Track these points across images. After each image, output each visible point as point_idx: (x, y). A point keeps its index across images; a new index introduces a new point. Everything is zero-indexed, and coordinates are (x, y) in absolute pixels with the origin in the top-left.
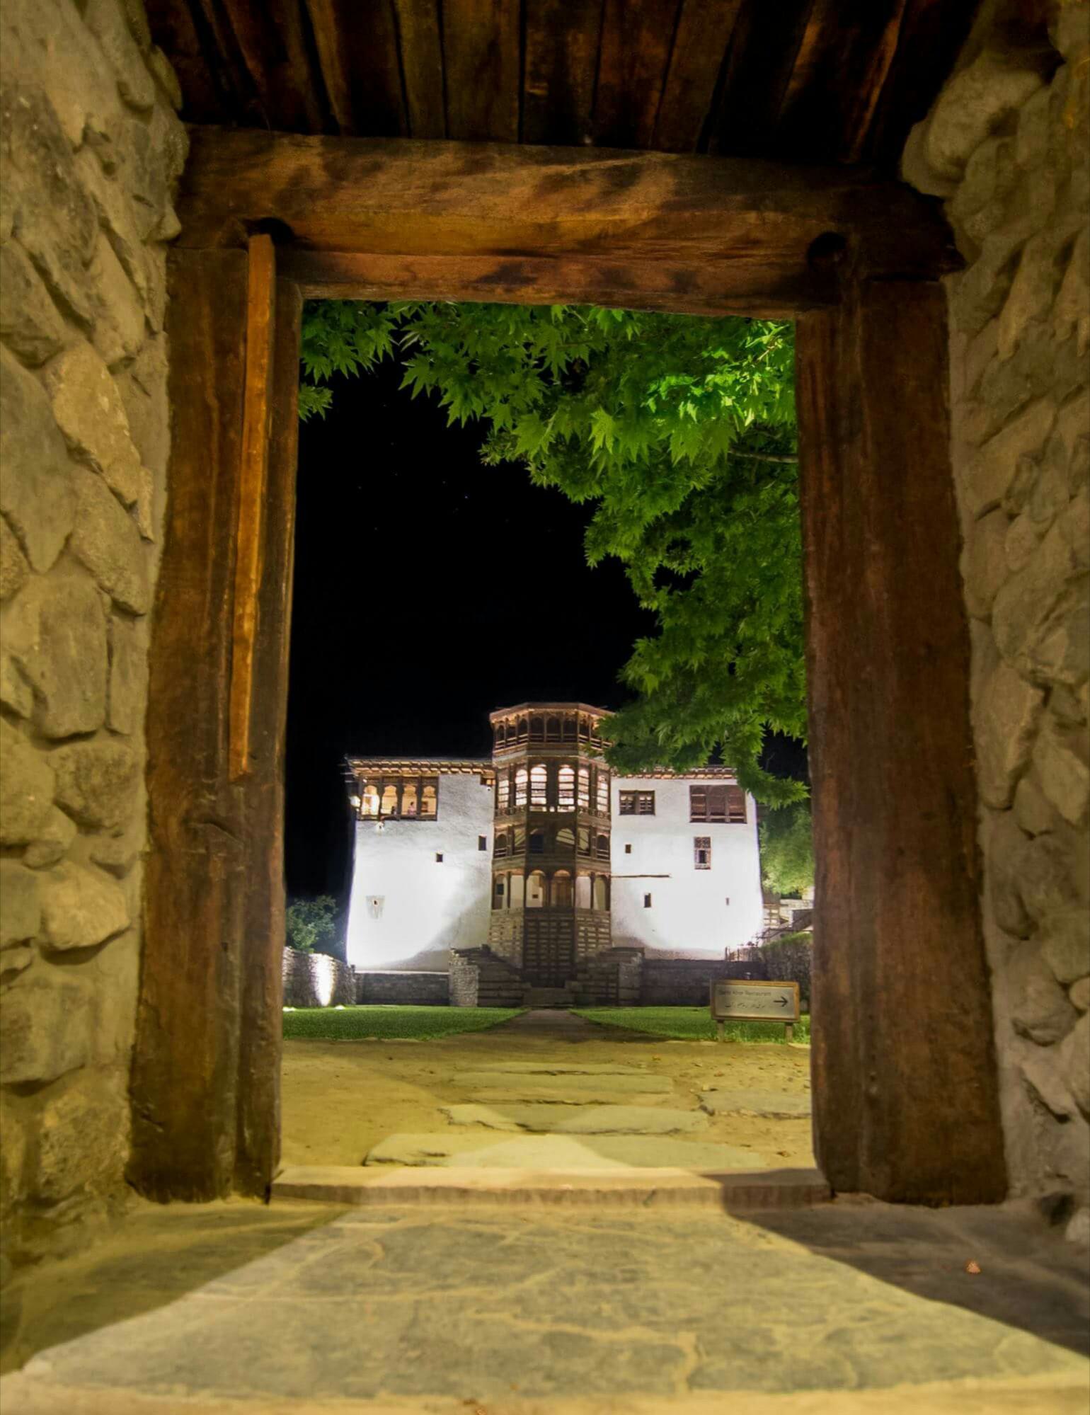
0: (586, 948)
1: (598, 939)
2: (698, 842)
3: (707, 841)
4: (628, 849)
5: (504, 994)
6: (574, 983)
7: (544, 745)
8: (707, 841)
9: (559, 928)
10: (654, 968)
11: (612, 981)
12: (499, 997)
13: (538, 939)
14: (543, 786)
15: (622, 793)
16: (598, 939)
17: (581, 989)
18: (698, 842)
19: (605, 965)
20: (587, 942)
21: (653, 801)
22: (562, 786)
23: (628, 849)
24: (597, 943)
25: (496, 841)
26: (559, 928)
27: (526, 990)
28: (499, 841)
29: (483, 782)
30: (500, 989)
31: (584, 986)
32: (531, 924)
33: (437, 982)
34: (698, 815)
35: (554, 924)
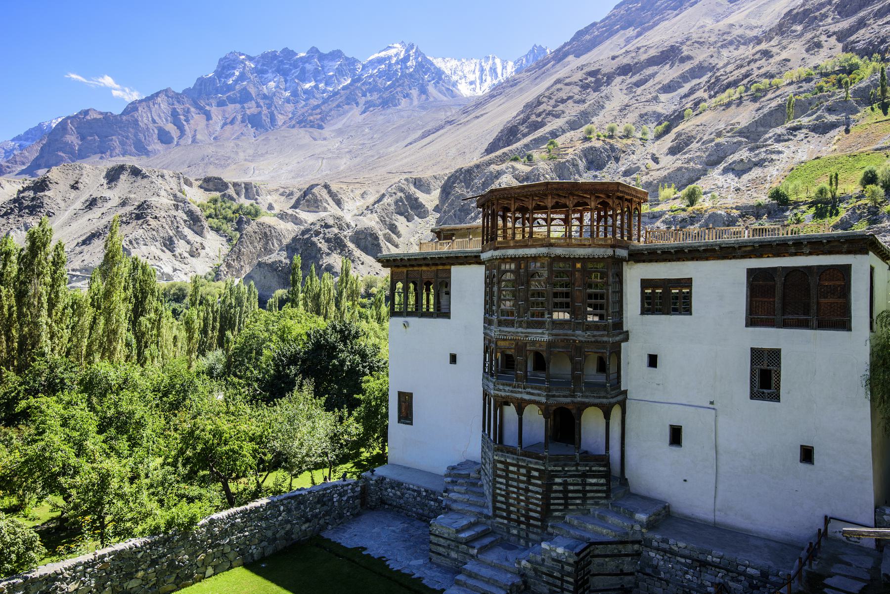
0: (566, 505)
1: (584, 492)
2: (757, 354)
3: (775, 355)
4: (653, 361)
5: (454, 555)
8: (775, 355)
9: (529, 477)
10: (658, 549)
11: (569, 574)
12: (448, 556)
16: (584, 492)
17: (532, 573)
18: (757, 354)
20: (566, 498)
21: (690, 294)
23: (653, 361)
24: (584, 499)
26: (529, 477)
30: (449, 547)
31: (535, 570)
32: (499, 465)
33: (436, 500)
34: (757, 316)
35: (523, 471)
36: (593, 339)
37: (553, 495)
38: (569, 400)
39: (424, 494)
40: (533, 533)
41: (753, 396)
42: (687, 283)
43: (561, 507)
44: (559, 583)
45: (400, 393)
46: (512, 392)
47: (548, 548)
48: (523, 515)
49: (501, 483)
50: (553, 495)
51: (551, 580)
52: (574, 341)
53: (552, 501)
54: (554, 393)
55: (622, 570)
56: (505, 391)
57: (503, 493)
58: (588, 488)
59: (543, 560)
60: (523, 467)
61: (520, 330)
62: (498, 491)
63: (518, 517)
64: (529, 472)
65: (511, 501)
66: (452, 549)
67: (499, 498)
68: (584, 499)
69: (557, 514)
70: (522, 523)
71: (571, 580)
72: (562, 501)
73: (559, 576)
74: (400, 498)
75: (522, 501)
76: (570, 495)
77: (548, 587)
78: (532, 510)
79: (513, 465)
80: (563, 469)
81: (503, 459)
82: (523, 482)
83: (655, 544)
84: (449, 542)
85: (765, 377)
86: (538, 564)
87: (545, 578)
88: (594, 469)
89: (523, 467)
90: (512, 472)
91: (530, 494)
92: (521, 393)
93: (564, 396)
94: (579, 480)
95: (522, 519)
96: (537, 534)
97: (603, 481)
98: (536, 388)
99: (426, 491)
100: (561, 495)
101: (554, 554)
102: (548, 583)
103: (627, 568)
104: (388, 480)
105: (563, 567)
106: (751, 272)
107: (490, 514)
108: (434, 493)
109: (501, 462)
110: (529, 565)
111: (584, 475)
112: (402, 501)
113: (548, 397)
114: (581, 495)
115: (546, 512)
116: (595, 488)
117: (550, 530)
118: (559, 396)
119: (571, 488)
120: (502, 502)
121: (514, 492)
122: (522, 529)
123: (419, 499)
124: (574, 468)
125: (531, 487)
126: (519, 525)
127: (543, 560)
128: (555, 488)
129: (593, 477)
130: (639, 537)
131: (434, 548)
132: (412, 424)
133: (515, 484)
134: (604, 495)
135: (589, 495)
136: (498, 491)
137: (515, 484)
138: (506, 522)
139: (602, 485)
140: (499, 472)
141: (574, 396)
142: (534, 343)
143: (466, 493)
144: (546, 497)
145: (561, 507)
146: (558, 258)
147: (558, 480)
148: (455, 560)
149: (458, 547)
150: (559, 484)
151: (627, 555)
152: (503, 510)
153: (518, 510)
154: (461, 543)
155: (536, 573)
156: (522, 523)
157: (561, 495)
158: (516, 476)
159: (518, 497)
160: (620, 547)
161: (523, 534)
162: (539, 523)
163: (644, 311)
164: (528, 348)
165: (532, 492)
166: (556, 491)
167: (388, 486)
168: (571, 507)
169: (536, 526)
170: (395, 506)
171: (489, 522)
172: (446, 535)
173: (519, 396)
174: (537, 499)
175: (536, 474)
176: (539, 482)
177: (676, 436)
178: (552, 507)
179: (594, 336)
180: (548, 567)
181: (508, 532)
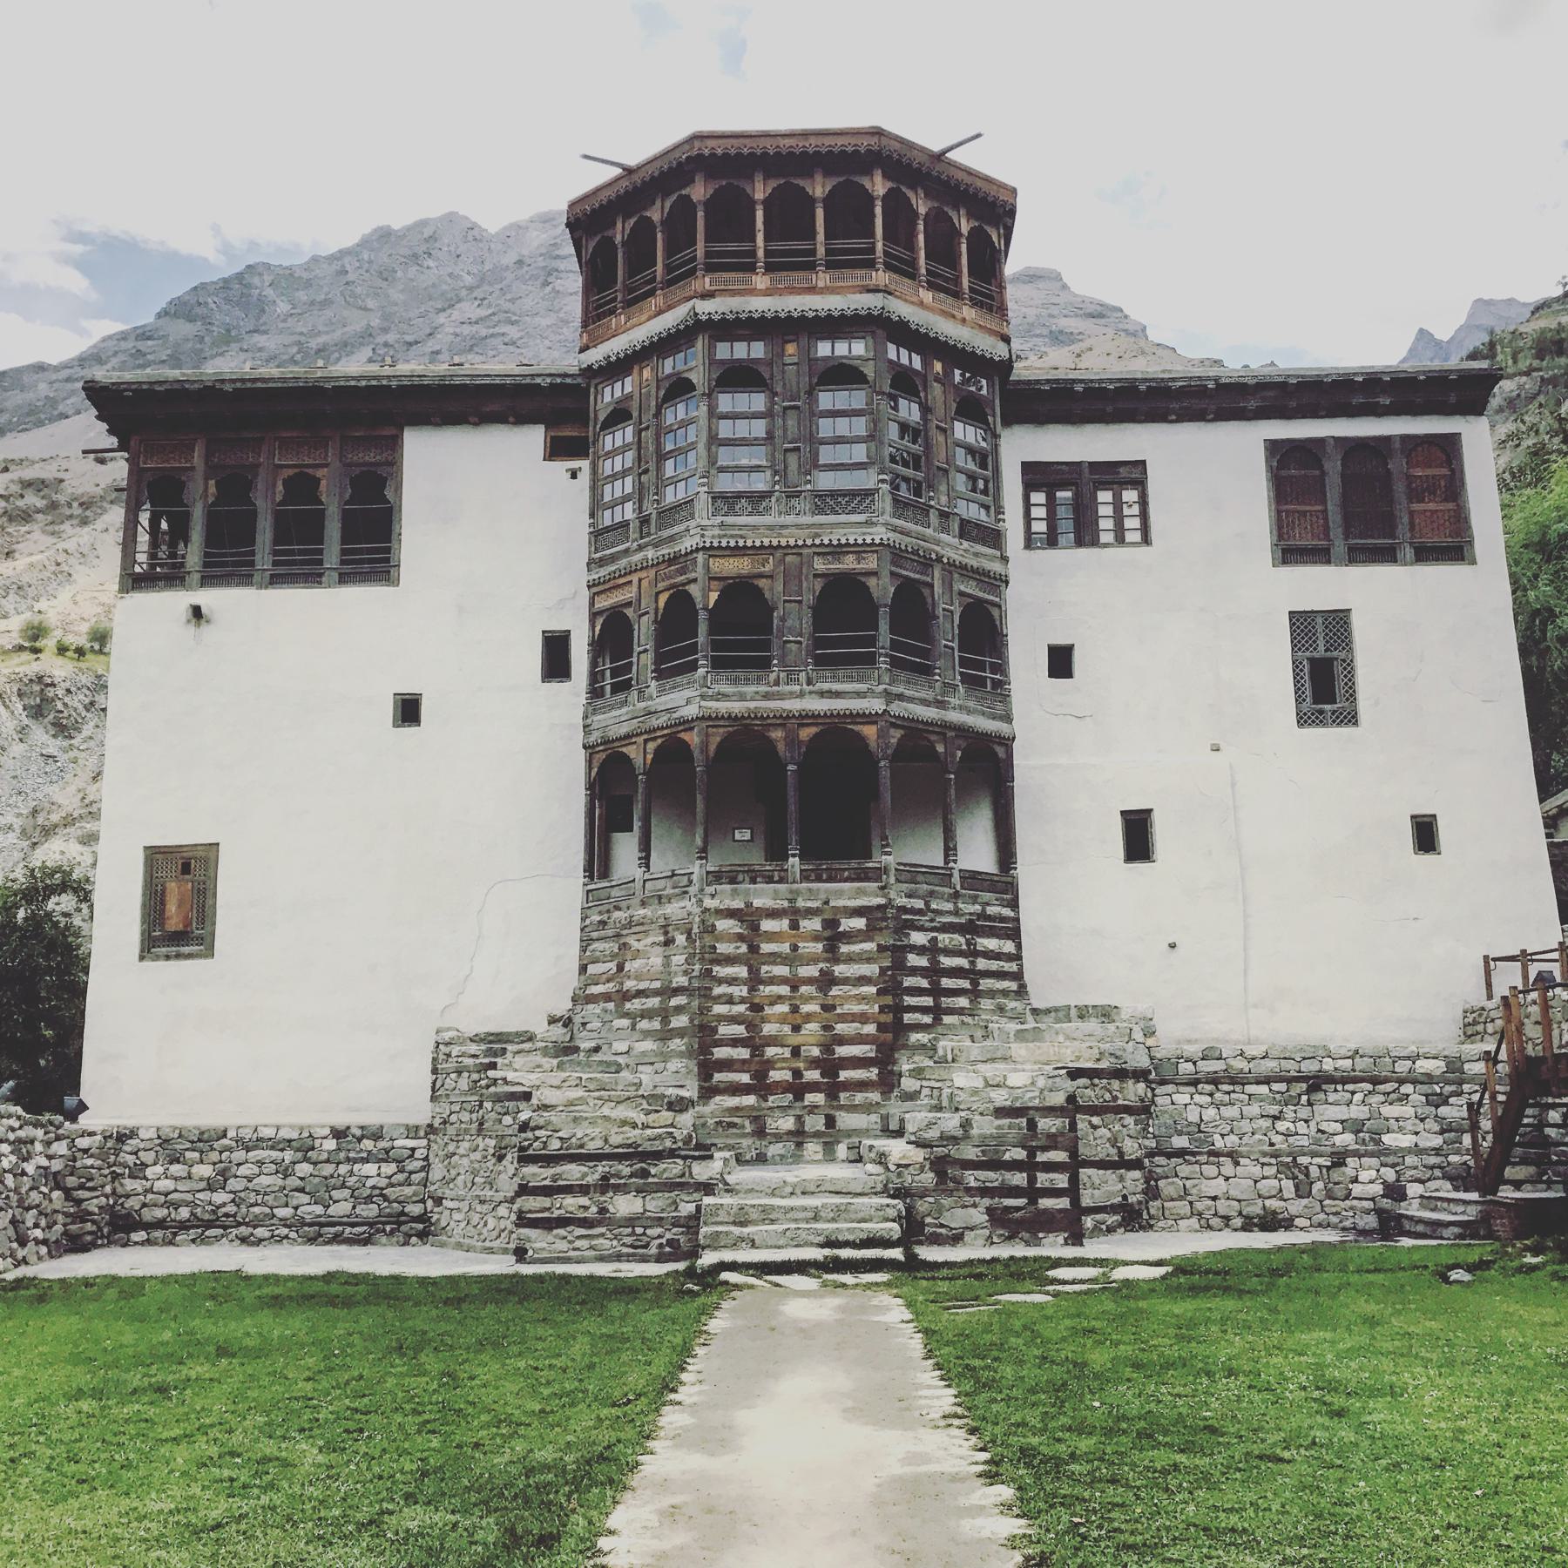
0: (937, 1012)
2: (1302, 623)
5: (625, 1205)
6: (898, 1149)
7: (761, 281)
9: (833, 938)
10: (1194, 1083)
11: (1052, 1142)
13: (755, 981)
14: (759, 428)
15: (1037, 475)
16: (973, 975)
17: (929, 1178)
18: (1302, 623)
19: (1017, 1079)
20: (936, 991)
22: (825, 428)
23: (1061, 662)
24: (975, 994)
25: (598, 648)
27: (707, 1188)
28: (612, 635)
29: (557, 450)
30: (605, 1185)
31: (940, 1165)
32: (723, 925)
33: (386, 1157)
35: (815, 924)
36: (974, 562)
37: (909, 982)
38: (930, 713)
39: (331, 1144)
40: (853, 1108)
41: (1303, 720)
42: (1131, 475)
43: (927, 1019)
44: (1019, 1179)
45: (155, 856)
46: (767, 696)
47: (980, 1084)
48: (814, 1063)
49: (732, 981)
50: (909, 982)
51: (992, 1177)
52: (939, 559)
53: (909, 1000)
54: (900, 689)
55: (1121, 1153)
56: (742, 697)
57: (741, 1008)
58: (982, 964)
59: (966, 1125)
60: (811, 913)
61: (790, 519)
62: (719, 1009)
63: (797, 1073)
64: (831, 924)
65: (769, 1029)
66: (617, 1189)
67: (725, 1030)
68: (975, 994)
69: (915, 1037)
70: (814, 1087)
71: (1059, 1156)
72: (928, 1001)
73: (1020, 1154)
74: (211, 1188)
75: (809, 1017)
76: (946, 983)
77: (986, 1202)
78: (842, 1041)
79: (773, 914)
80: (927, 904)
81: (738, 904)
82: (813, 960)
83: (1186, 1068)
84: (602, 1168)
85: (1324, 679)
86: (955, 1140)
87: (971, 1178)
88: (991, 910)
89: (811, 913)
90: (772, 937)
91: (835, 991)
92: (801, 695)
93: (925, 702)
94: (959, 940)
95: (813, 1075)
96: (868, 1108)
97: (1009, 947)
98: (850, 679)
99: (339, 1134)
100: (924, 983)
101: (1000, 1098)
102: (984, 1191)
103: (1131, 1148)
104: (143, 1134)
105: (1032, 1125)
106: (1273, 447)
107: (691, 1092)
108: (377, 1136)
109: (731, 914)
110: (918, 1155)
111: (970, 928)
112: (220, 1197)
113: (889, 697)
114: (966, 984)
115: (893, 1035)
116: (994, 965)
117: (908, 1084)
118: (911, 700)
119: (947, 962)
120: (735, 1042)
121: (779, 999)
122: (813, 1109)
123: (304, 1169)
124: (949, 906)
125: (840, 970)
126: (799, 1097)
127: (966, 1125)
128: (914, 960)
129: (992, 933)
130: (1143, 1062)
131: (532, 1203)
132: (209, 952)
133: (782, 970)
134: (1013, 986)
135: (986, 984)
136: (719, 1009)
137: (782, 970)
138: (750, 1100)
139: (1010, 958)
140: (724, 948)
141: (941, 704)
142: (838, 551)
143: (560, 1066)
144: (891, 986)
145: (927, 1019)
146: (902, 333)
147: (918, 938)
148: (631, 1221)
149: (645, 1174)
150: (921, 950)
151: (1128, 1110)
152: (741, 1066)
153: (796, 1052)
154: (658, 1156)
155: (941, 1175)
156: (814, 1087)
157: (924, 983)
158: (785, 948)
159: (795, 1009)
160: (1116, 1084)
161: (815, 1123)
162: (873, 1073)
163: (1029, 545)
164: (820, 565)
165: (845, 981)
166: (914, 971)
167: (148, 1157)
168: (947, 1019)
169: (862, 1086)
170: (184, 1226)
171: (686, 1119)
172: (593, 1146)
173: (794, 705)
174: (863, 999)
175: (859, 923)
176: (870, 946)
177: (1138, 836)
178: (908, 1018)
179: (976, 555)
180: (983, 1143)
181: (760, 1132)
